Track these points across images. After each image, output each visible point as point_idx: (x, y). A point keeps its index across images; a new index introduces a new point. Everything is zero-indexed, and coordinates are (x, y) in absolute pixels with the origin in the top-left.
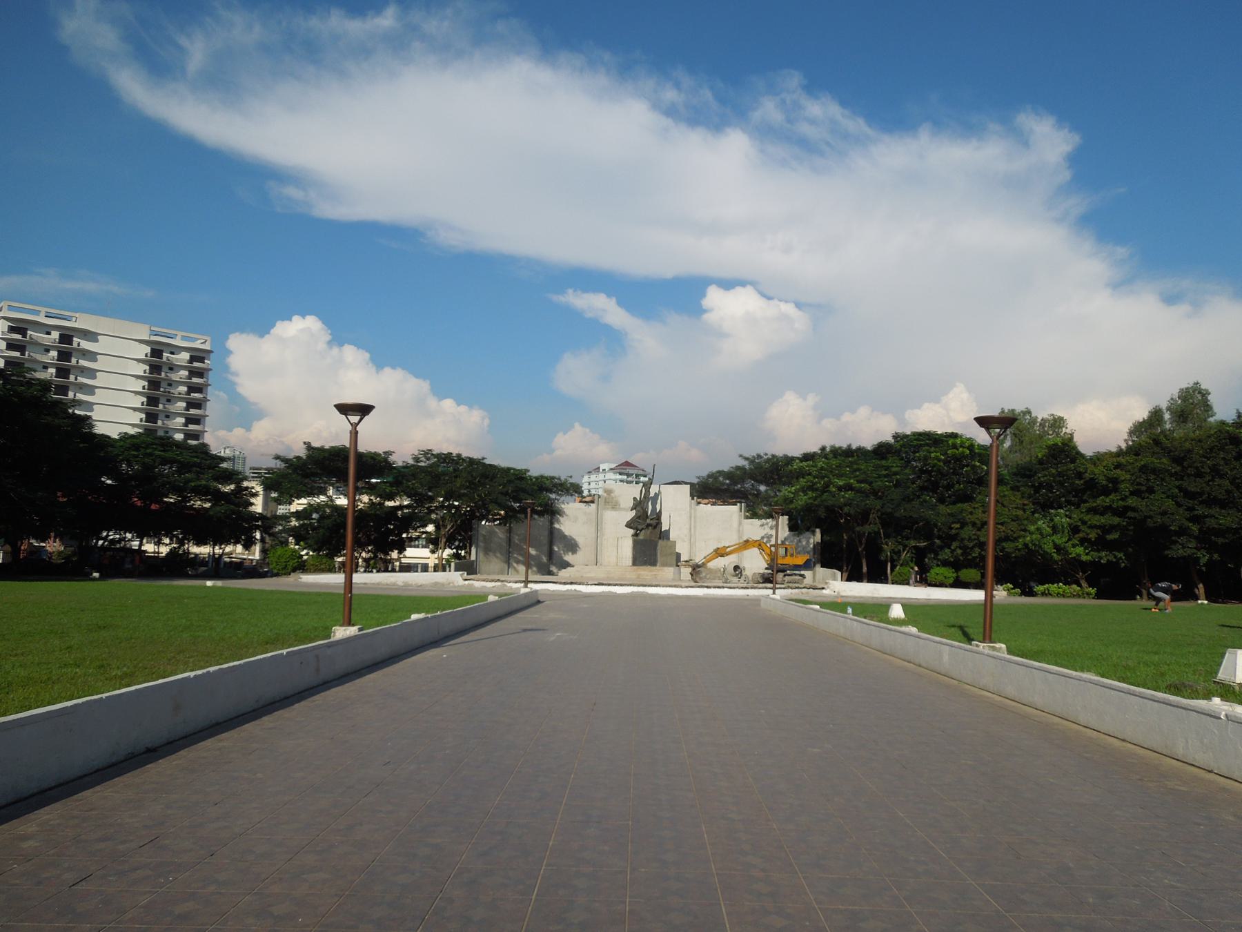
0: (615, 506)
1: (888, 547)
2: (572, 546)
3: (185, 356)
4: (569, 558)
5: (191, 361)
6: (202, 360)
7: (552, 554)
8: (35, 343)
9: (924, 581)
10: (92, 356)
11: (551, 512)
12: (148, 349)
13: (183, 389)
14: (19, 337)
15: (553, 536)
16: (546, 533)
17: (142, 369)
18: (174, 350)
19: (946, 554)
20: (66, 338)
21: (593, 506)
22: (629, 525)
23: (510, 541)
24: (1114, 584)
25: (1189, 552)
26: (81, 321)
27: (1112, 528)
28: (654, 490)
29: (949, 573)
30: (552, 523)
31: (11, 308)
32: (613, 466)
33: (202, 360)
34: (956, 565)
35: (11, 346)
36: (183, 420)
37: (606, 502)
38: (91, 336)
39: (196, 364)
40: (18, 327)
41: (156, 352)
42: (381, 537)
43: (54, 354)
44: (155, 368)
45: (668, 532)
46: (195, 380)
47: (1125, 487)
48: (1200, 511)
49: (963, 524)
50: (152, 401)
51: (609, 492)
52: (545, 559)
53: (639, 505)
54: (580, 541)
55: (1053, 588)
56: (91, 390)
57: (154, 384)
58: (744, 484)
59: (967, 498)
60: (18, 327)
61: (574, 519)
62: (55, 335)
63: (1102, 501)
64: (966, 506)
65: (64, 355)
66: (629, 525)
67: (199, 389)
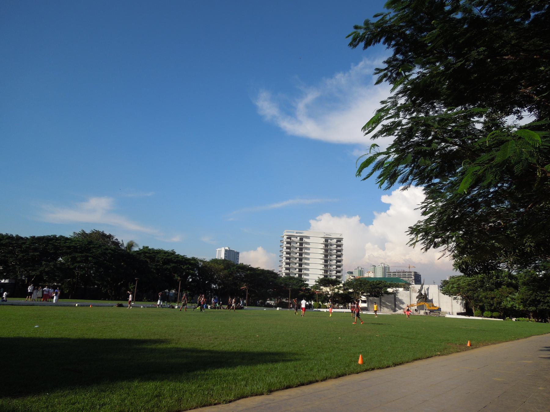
2: (403, 303)
3: (335, 240)
4: (401, 306)
5: (337, 242)
6: (340, 241)
8: (293, 242)
9: (482, 315)
12: (324, 240)
13: (335, 251)
14: (289, 240)
15: (395, 299)
16: (393, 300)
17: (323, 246)
18: (332, 239)
20: (301, 239)
21: (408, 292)
23: (381, 301)
25: (544, 307)
26: (305, 234)
29: (489, 313)
30: (395, 296)
31: (287, 232)
33: (340, 241)
34: (492, 311)
35: (288, 243)
37: (413, 290)
38: (308, 237)
39: (339, 243)
40: (289, 237)
41: (326, 241)
43: (298, 244)
44: (326, 245)
46: (338, 248)
50: (326, 256)
52: (394, 306)
53: (420, 291)
54: (404, 301)
56: (308, 254)
57: (326, 251)
59: (492, 290)
60: (289, 237)
62: (298, 238)
65: (301, 244)
67: (340, 251)
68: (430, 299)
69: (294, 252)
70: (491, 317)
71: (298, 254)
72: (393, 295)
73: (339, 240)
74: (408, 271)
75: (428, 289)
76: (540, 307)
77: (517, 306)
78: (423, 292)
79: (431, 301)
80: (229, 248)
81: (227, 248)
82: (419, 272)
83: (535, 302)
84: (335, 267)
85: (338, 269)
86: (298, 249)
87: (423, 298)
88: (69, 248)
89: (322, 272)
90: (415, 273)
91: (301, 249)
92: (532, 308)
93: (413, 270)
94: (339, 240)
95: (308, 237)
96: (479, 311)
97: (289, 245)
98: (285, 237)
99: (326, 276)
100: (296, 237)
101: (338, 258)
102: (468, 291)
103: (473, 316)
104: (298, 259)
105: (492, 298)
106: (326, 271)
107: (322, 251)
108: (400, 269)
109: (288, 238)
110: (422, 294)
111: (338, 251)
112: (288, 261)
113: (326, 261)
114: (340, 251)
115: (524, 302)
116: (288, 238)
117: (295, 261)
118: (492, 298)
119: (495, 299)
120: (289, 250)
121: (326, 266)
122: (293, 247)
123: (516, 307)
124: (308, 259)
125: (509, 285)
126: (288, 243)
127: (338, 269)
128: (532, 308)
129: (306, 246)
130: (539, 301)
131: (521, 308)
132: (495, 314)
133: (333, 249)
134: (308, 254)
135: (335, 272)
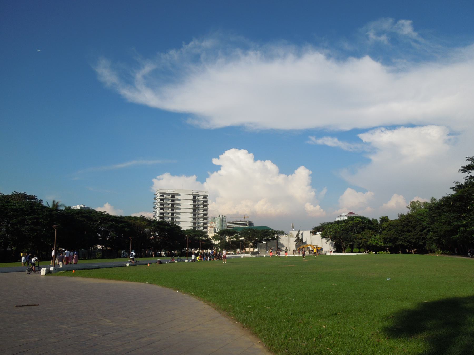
0: (293, 237)
1: (344, 244)
2: (284, 246)
3: (202, 197)
6: (206, 198)
7: (278, 248)
8: (166, 199)
9: (352, 252)
10: (179, 200)
11: (277, 239)
13: (202, 206)
14: (162, 197)
15: (278, 243)
18: (199, 196)
19: (356, 245)
20: (173, 196)
22: (295, 241)
24: (394, 250)
25: (400, 243)
27: (387, 238)
28: (301, 232)
29: (357, 250)
32: (346, 214)
33: (206, 198)
35: (161, 200)
36: (202, 215)
37: (291, 236)
38: (179, 195)
40: (162, 195)
41: (194, 197)
42: (241, 246)
43: (170, 200)
44: (194, 201)
45: (306, 242)
46: (205, 203)
47: (387, 229)
48: (402, 234)
49: (356, 239)
50: (194, 210)
51: (291, 233)
53: (297, 236)
55: (380, 252)
57: (194, 206)
58: (324, 230)
60: (162, 195)
61: (283, 239)
62: (171, 196)
63: (383, 232)
64: (358, 235)
65: (173, 201)
66: (295, 241)
67: (206, 206)
68: (304, 241)
69: (166, 208)
70: (359, 252)
71: (170, 209)
72: (275, 241)
73: (205, 197)
74: (244, 220)
75: (302, 235)
76: (398, 243)
77: (380, 244)
78: (300, 237)
79: (305, 243)
80: (84, 206)
81: (82, 206)
82: (252, 221)
83: (393, 240)
84: (202, 219)
85: (205, 221)
86: (170, 205)
87: (299, 241)
88: (16, 210)
89: (191, 224)
90: (249, 222)
91: (173, 205)
92: (390, 244)
93: (247, 219)
94: (205, 197)
95: (179, 195)
96: (350, 249)
97: (162, 202)
98: (159, 195)
99: (195, 228)
100: (169, 194)
101: (205, 212)
102: (343, 234)
103: (341, 252)
104: (170, 214)
105: (361, 239)
106: (194, 223)
107: (191, 206)
108: (238, 219)
109: (161, 196)
110: (299, 238)
111: (204, 206)
112: (162, 216)
113: (194, 215)
114: (204, 206)
115: (385, 241)
116: (161, 196)
117: (168, 216)
118: (361, 239)
119: (363, 239)
120: (162, 206)
121: (194, 219)
122: (166, 203)
123: (378, 244)
124: (179, 213)
125: (370, 228)
126: (161, 200)
127: (205, 221)
128: (390, 244)
129: (177, 202)
130: (398, 239)
131: (383, 244)
132: (361, 250)
133: (200, 204)
134: (179, 209)
135: (202, 224)
